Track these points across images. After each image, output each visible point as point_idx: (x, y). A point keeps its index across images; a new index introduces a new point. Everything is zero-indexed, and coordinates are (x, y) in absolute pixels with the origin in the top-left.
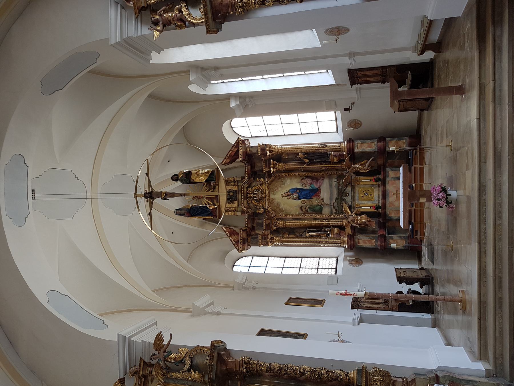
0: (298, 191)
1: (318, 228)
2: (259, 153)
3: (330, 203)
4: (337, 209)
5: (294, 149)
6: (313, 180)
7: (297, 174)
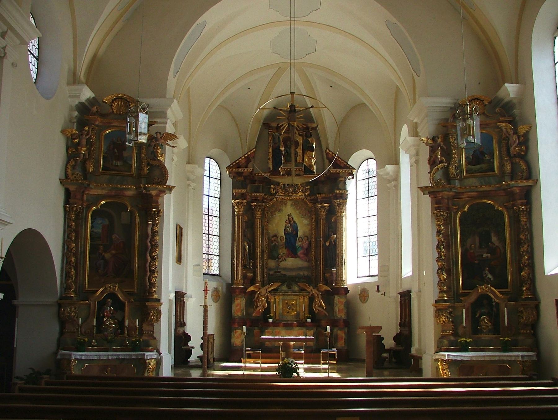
0: (294, 232)
1: (252, 255)
2: (338, 192)
3: (280, 269)
5: (341, 230)
6: (307, 249)
7: (314, 232)
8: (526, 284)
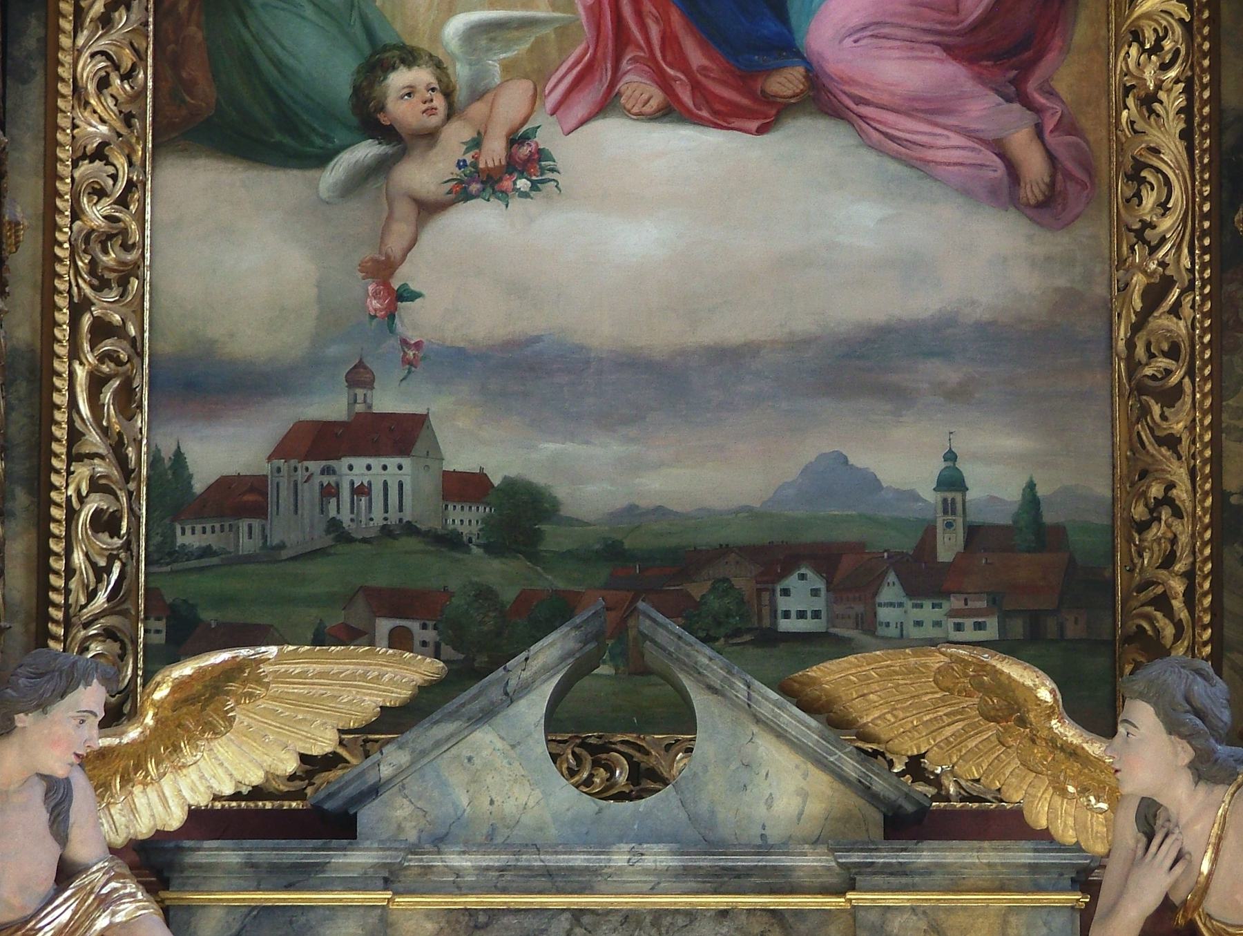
4: (259, 511)
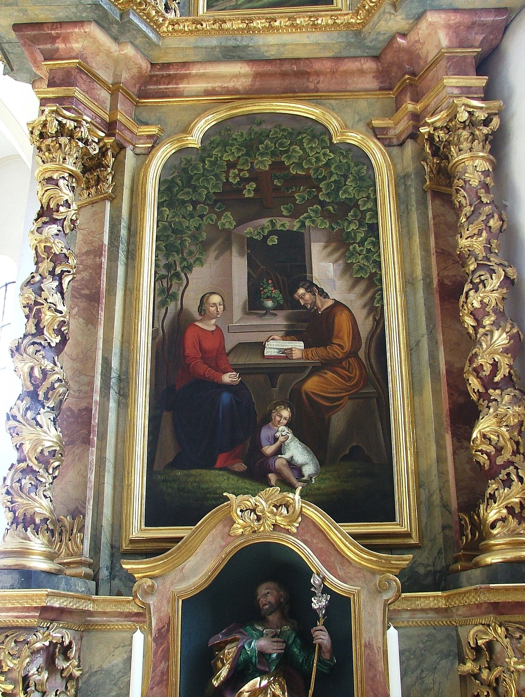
8: (507, 483)
